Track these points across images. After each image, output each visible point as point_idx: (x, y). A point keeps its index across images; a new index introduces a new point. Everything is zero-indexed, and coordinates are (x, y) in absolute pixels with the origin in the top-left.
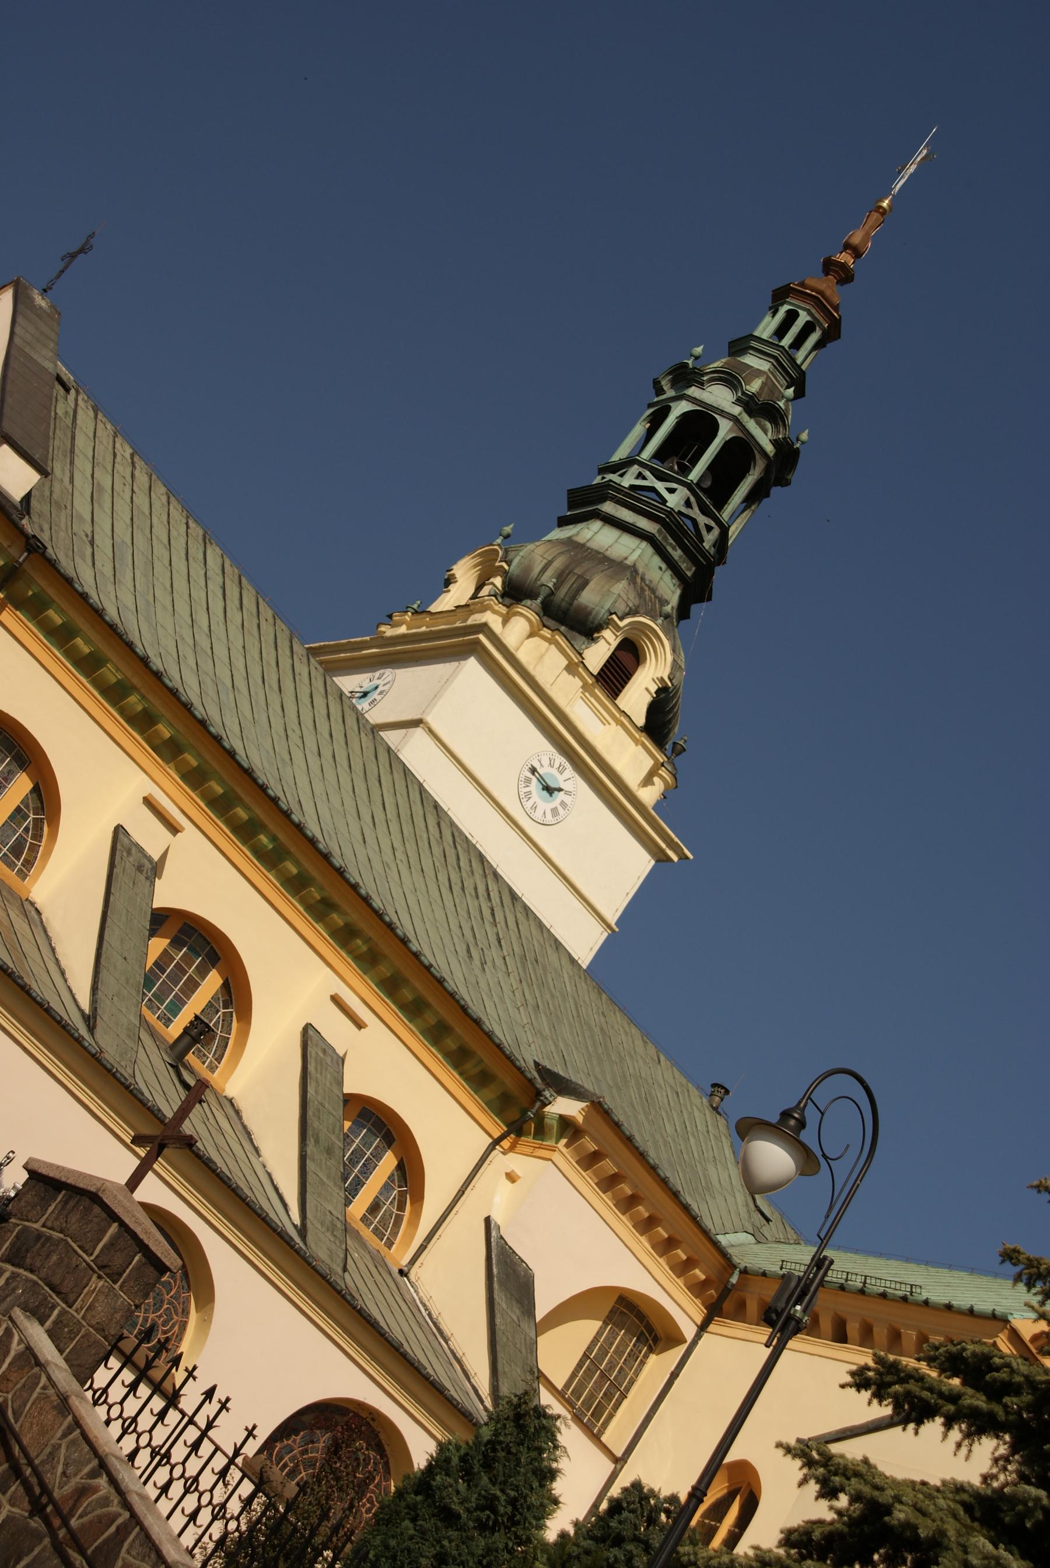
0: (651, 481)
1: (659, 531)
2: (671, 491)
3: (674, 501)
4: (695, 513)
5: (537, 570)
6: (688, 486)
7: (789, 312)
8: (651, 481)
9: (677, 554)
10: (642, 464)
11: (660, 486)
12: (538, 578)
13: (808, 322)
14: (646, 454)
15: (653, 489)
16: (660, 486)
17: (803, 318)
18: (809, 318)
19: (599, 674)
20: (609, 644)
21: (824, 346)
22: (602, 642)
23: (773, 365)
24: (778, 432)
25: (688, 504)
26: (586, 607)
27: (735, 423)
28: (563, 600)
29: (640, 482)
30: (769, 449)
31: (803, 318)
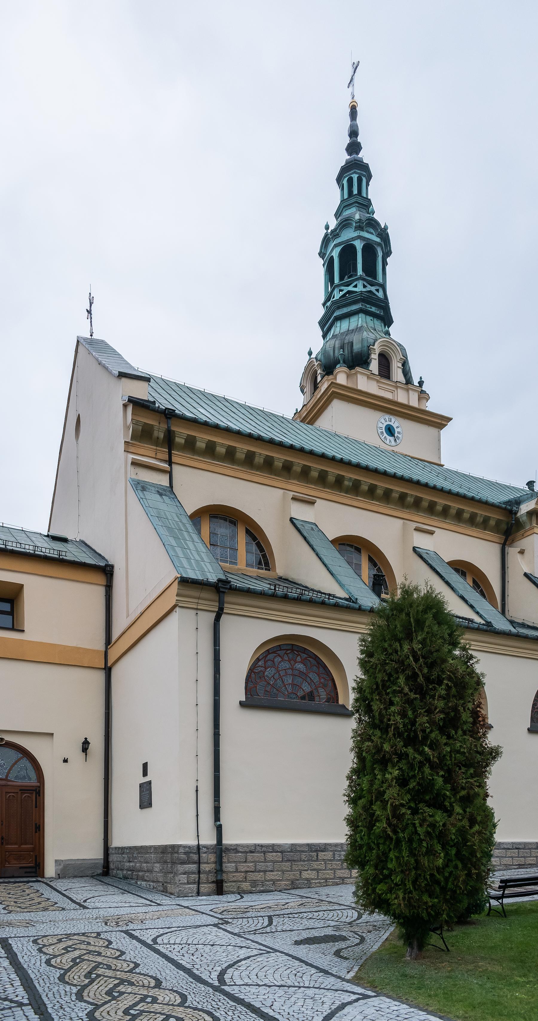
0: (346, 289)
1: (362, 305)
2: (356, 286)
3: (360, 288)
4: (369, 288)
5: (332, 353)
6: (361, 278)
7: (348, 180)
8: (346, 289)
9: (373, 309)
10: (338, 286)
11: (351, 288)
12: (334, 358)
13: (357, 177)
14: (337, 280)
15: (349, 292)
16: (351, 288)
17: (355, 177)
18: (357, 175)
19: (379, 373)
20: (376, 359)
21: (369, 185)
22: (373, 361)
23: (357, 206)
24: (377, 230)
25: (365, 286)
26: (358, 352)
27: (361, 239)
28: (348, 357)
29: (342, 293)
30: (378, 240)
31: (355, 177)
